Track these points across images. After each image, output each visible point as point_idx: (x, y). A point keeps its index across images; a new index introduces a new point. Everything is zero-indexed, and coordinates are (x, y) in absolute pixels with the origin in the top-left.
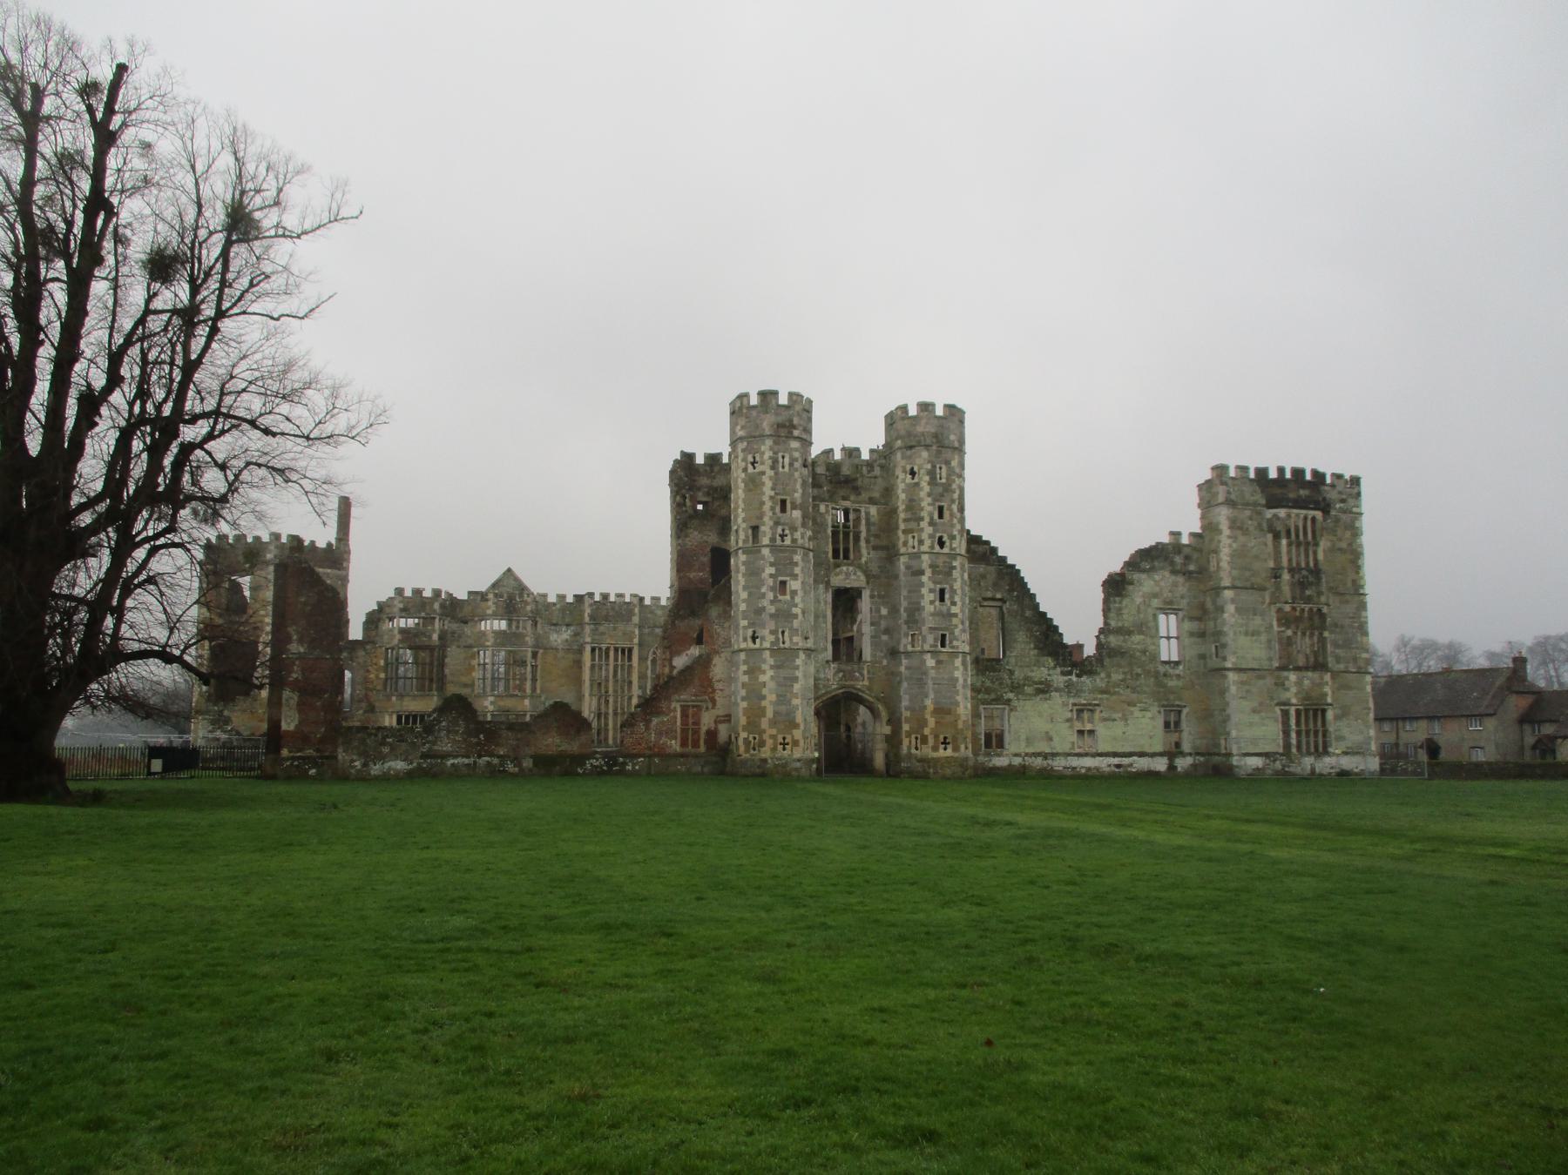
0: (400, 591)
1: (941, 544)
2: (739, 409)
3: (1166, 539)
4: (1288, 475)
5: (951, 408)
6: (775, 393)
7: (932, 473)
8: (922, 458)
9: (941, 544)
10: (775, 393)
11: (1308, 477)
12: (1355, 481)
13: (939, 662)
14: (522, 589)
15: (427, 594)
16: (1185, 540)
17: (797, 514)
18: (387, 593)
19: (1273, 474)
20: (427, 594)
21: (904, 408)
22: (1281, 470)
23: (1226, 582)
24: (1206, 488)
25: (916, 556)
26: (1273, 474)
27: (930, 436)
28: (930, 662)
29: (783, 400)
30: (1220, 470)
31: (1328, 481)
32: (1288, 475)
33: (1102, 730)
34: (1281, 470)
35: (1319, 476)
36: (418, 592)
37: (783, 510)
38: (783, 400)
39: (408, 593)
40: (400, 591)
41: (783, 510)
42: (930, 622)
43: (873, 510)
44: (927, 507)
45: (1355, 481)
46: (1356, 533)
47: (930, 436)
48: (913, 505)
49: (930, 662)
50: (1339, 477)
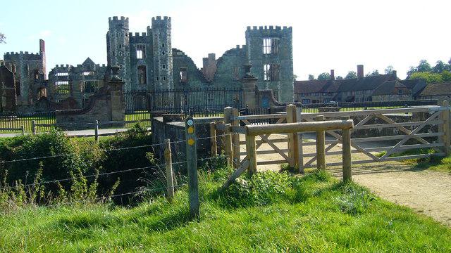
0: (57, 66)
1: (164, 54)
2: (110, 22)
3: (235, 47)
4: (268, 28)
5: (166, 18)
6: (117, 17)
7: (160, 35)
8: (158, 32)
9: (164, 54)
10: (117, 17)
11: (274, 28)
12: (291, 28)
13: (163, 84)
14: (93, 63)
15: (65, 66)
16: (241, 47)
17: (124, 48)
18: (54, 67)
19: (264, 28)
20: (65, 66)
21: (153, 18)
22: (266, 27)
23: (250, 58)
24: (246, 33)
25: (157, 57)
26: (264, 28)
27: (161, 26)
28: (161, 84)
29: (119, 19)
30: (249, 28)
31: (282, 28)
32: (268, 28)
33: (215, 99)
34: (266, 27)
35: (278, 28)
36: (62, 65)
37: (120, 47)
38: (119, 19)
39: (60, 66)
40: (57, 66)
41: (120, 47)
42: (160, 73)
43: (148, 45)
44: (160, 45)
45: (291, 28)
46: (291, 42)
47: (161, 26)
48: (156, 43)
49: (161, 84)
50: (285, 27)
